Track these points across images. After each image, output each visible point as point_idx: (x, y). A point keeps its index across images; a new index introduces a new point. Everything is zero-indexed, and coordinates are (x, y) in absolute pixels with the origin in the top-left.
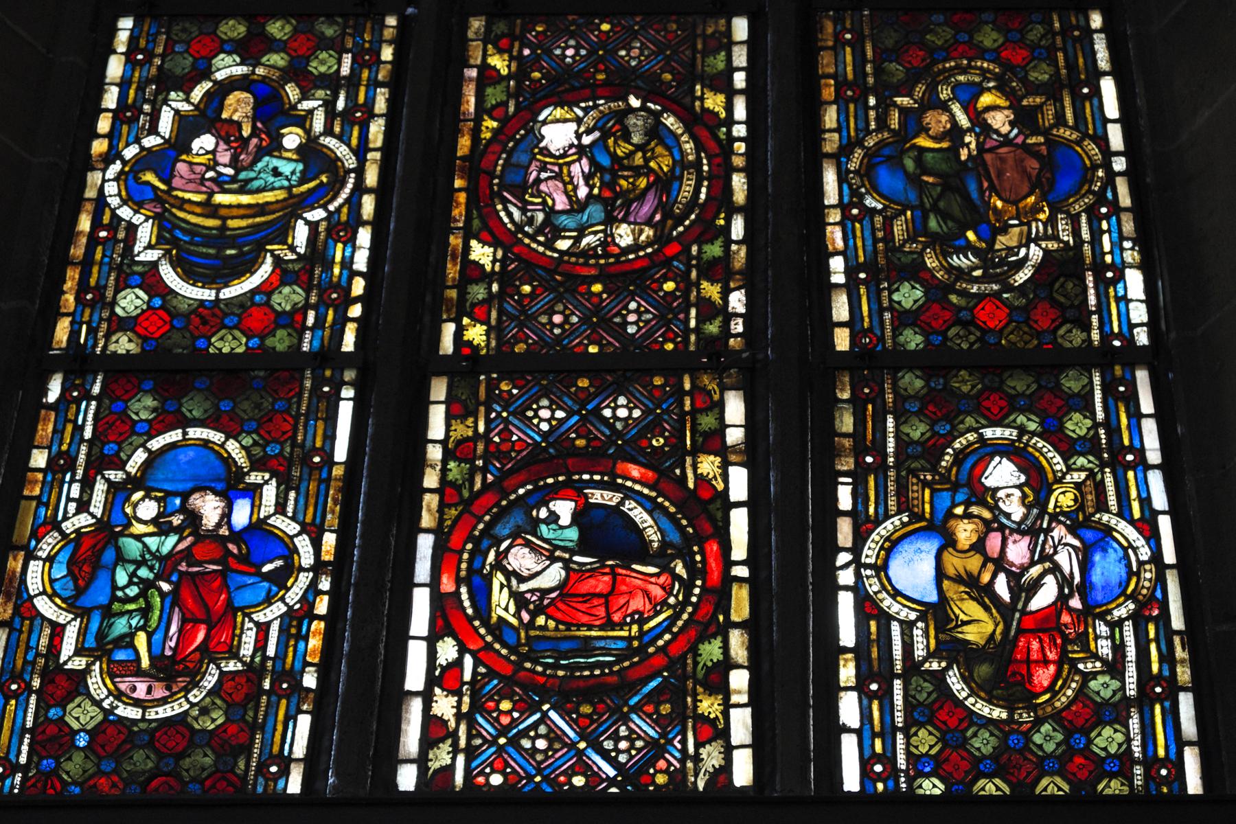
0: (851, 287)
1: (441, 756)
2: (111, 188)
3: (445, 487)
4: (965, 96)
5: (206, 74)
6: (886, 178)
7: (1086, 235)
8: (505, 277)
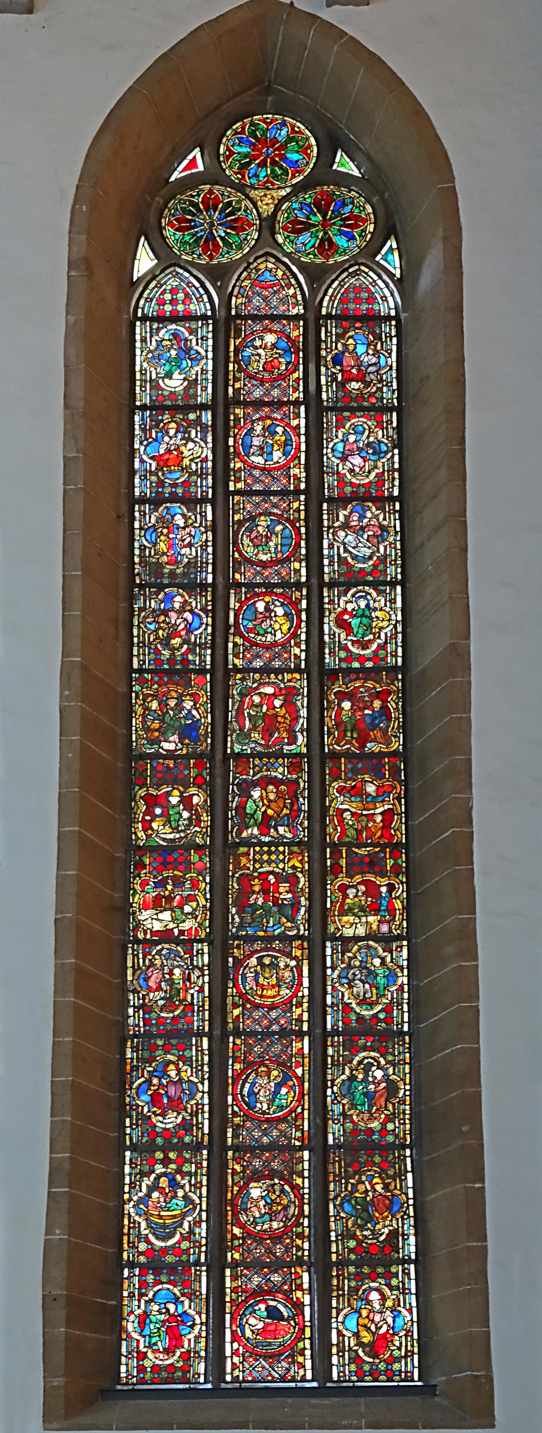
0: (336, 1241)
1: (236, 1373)
2: (132, 1210)
3: (232, 1301)
4: (369, 1179)
5: (153, 1172)
6: (347, 1207)
7: (400, 1225)
8: (243, 1238)
